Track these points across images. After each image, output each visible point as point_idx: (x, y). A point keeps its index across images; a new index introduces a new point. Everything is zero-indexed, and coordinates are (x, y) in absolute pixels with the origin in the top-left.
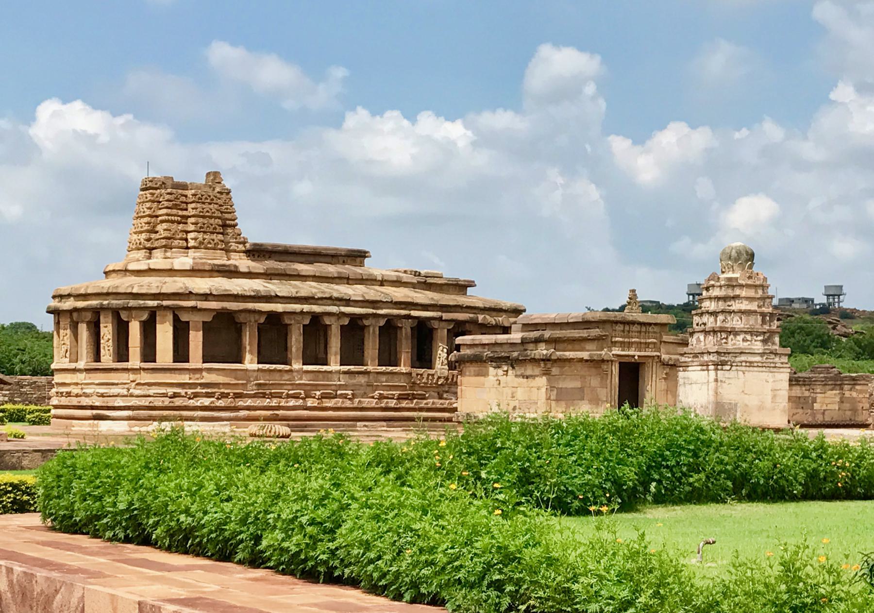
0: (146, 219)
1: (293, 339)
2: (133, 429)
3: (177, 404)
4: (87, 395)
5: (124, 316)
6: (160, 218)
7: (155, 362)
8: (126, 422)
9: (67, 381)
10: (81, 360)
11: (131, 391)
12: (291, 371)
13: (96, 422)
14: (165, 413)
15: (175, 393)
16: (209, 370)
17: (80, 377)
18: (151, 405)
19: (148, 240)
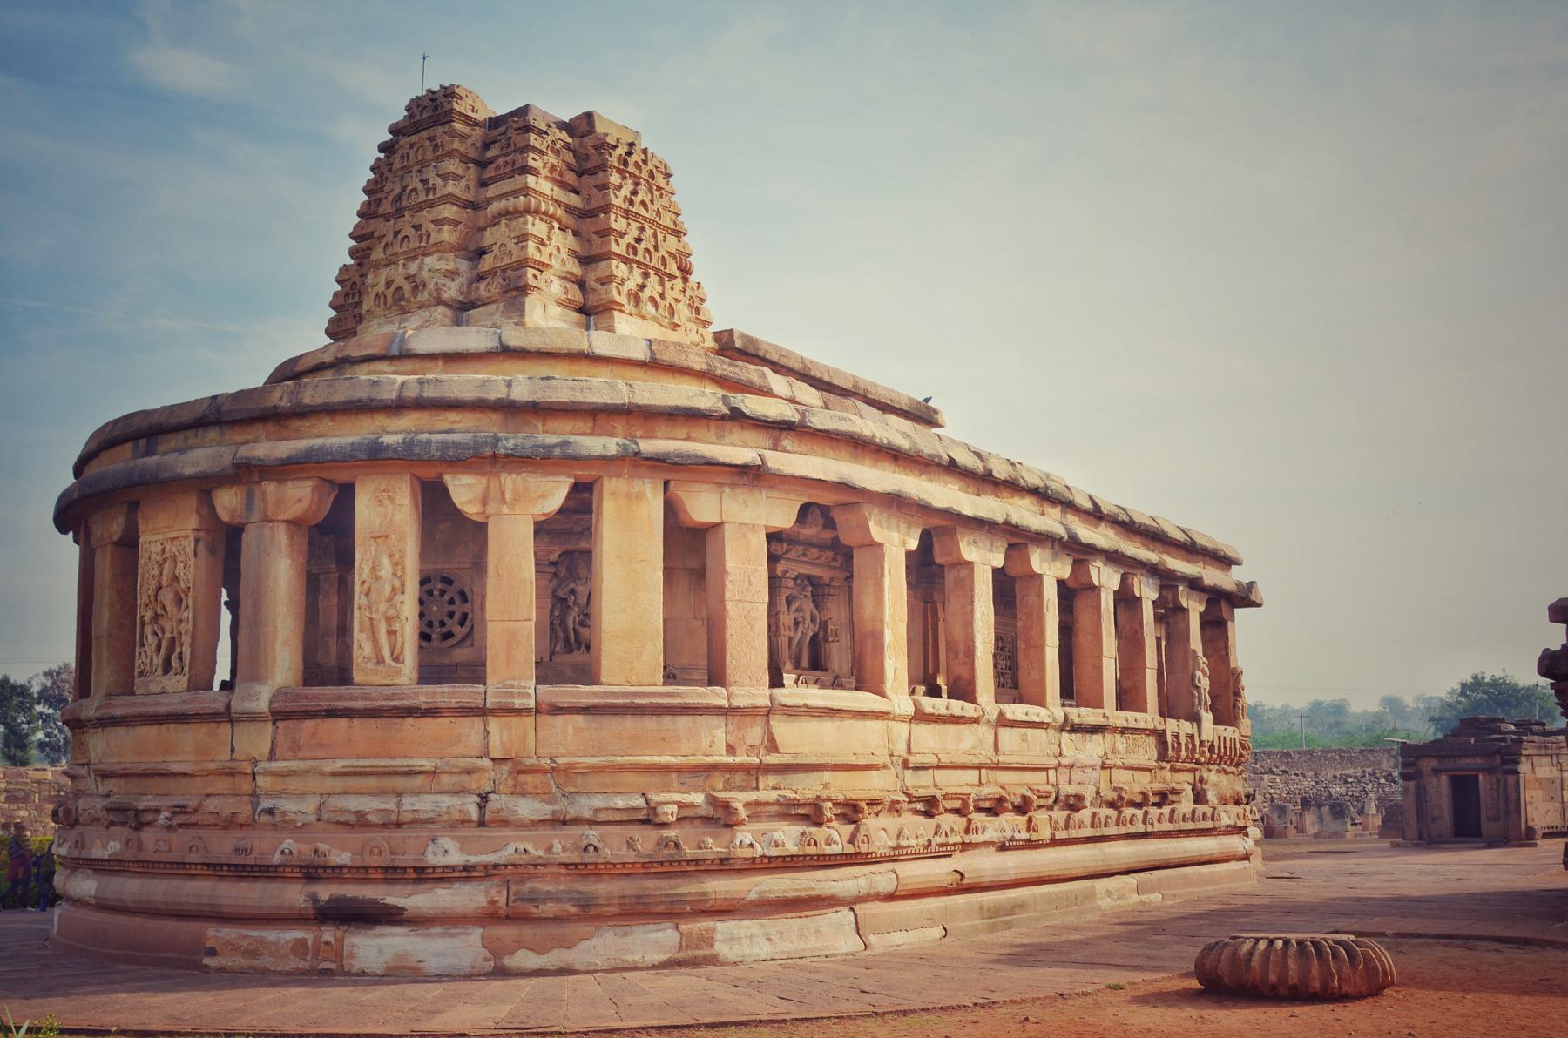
0: (449, 211)
1: (978, 614)
2: (508, 962)
3: (689, 851)
4: (286, 825)
5: (464, 491)
6: (495, 207)
7: (597, 682)
8: (476, 934)
9: (175, 768)
11: (495, 802)
12: (975, 721)
13: (328, 934)
14: (651, 885)
15: (681, 805)
16: (792, 712)
17: (255, 741)
18: (590, 857)
19: (452, 274)
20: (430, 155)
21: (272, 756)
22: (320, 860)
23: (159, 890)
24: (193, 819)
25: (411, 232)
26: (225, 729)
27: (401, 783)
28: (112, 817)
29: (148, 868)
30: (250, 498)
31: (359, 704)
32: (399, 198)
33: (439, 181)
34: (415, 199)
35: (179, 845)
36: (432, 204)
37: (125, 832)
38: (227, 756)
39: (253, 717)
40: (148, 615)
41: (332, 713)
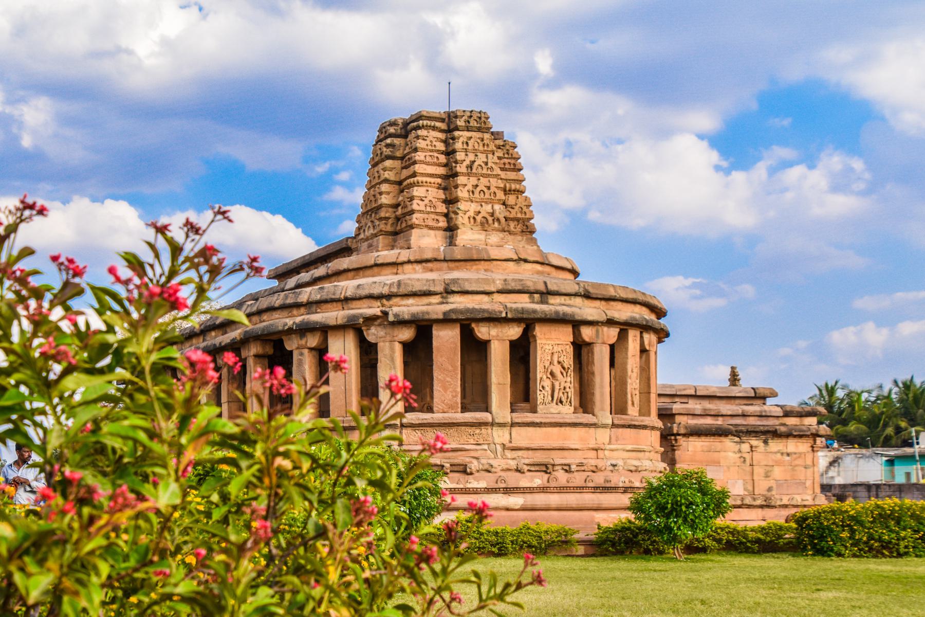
10: (602, 409)
17: (602, 436)
20: (481, 148)
21: (610, 443)
22: (633, 485)
23: (572, 499)
24: (583, 468)
25: (485, 190)
26: (592, 430)
27: (641, 455)
28: (529, 468)
29: (562, 490)
30: (597, 331)
31: (636, 423)
32: (470, 167)
33: (493, 166)
34: (480, 171)
35: (578, 479)
36: (488, 176)
37: (546, 476)
38: (594, 442)
39: (604, 426)
40: (545, 377)
41: (630, 426)
